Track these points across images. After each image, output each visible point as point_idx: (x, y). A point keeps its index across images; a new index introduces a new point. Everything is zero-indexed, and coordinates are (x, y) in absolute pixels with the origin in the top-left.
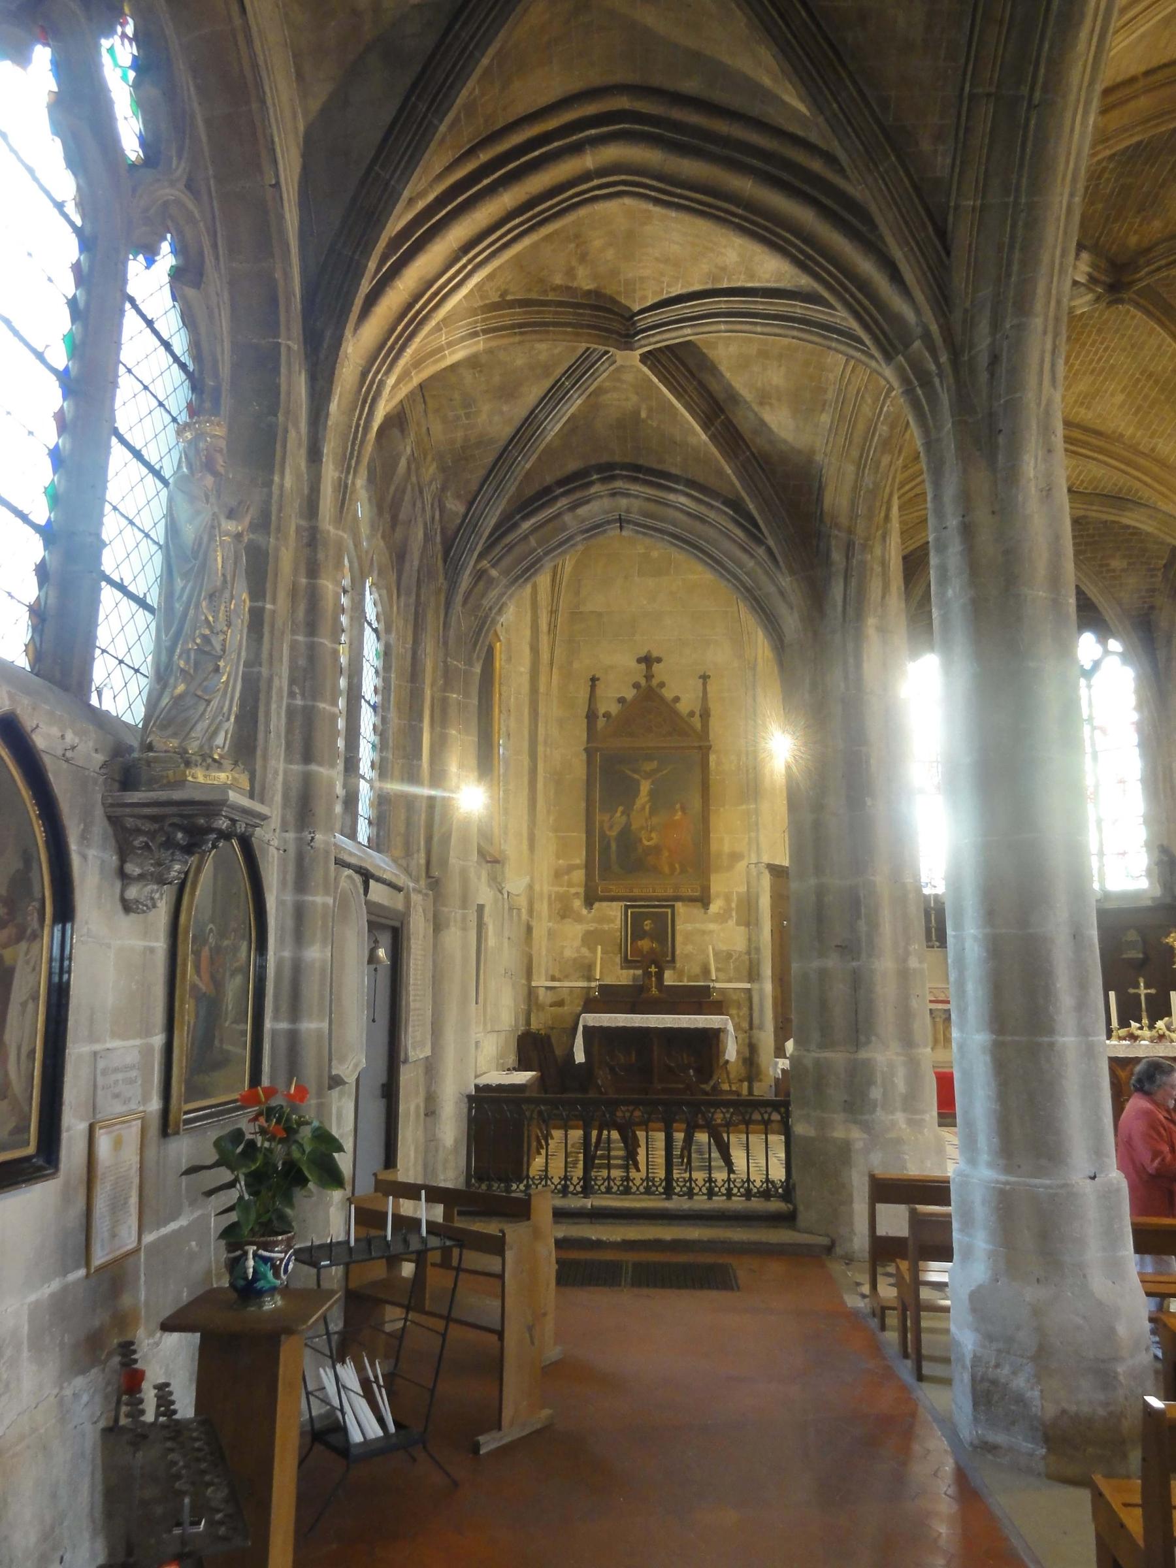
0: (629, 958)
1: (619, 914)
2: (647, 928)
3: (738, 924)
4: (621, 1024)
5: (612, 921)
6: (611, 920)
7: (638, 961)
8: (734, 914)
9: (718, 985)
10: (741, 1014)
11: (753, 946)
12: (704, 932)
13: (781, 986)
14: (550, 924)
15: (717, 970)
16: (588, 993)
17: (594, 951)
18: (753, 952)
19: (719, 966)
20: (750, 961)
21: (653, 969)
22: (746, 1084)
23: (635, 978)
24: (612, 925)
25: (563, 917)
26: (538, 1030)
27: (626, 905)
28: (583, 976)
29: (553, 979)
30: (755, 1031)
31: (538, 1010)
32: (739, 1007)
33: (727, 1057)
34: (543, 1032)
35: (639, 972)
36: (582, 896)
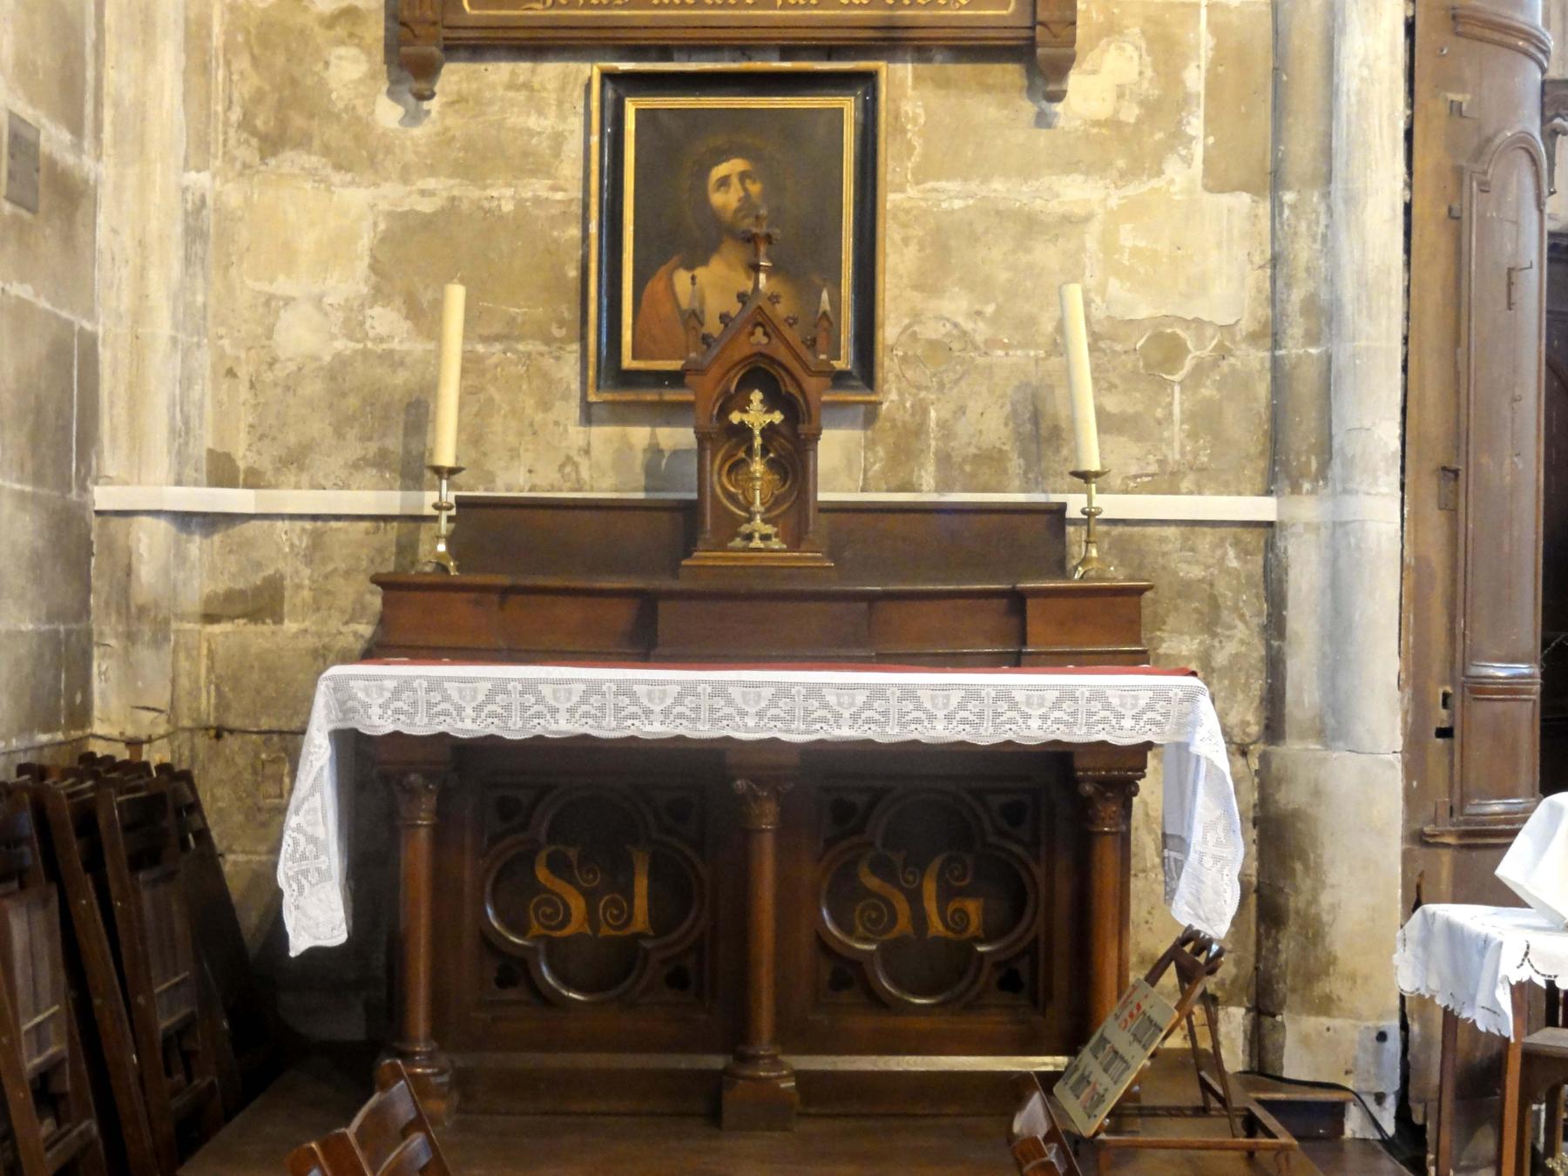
0: (628, 362)
1: (576, 123)
2: (725, 200)
3: (1217, 181)
4: (562, 726)
5: (530, 164)
6: (530, 164)
7: (675, 379)
8: (1195, 125)
9: (1112, 505)
10: (1220, 659)
11: (1297, 296)
12: (1030, 226)
13: (1451, 509)
14: (200, 180)
15: (1107, 423)
16: (406, 548)
17: (425, 317)
18: (1296, 329)
19: (1112, 404)
20: (1279, 373)
21: (757, 415)
22: (1234, 1021)
23: (656, 465)
24: (538, 187)
25: (272, 144)
26: (134, 744)
27: (608, 77)
28: (381, 461)
29: (222, 472)
30: (1294, 748)
31: (131, 637)
32: (1211, 621)
33: (1184, 914)
34: (155, 756)
35: (679, 437)
36: (376, 30)
